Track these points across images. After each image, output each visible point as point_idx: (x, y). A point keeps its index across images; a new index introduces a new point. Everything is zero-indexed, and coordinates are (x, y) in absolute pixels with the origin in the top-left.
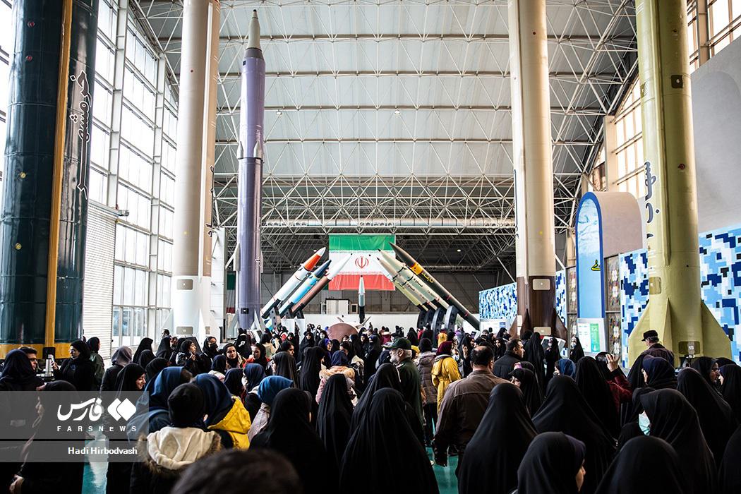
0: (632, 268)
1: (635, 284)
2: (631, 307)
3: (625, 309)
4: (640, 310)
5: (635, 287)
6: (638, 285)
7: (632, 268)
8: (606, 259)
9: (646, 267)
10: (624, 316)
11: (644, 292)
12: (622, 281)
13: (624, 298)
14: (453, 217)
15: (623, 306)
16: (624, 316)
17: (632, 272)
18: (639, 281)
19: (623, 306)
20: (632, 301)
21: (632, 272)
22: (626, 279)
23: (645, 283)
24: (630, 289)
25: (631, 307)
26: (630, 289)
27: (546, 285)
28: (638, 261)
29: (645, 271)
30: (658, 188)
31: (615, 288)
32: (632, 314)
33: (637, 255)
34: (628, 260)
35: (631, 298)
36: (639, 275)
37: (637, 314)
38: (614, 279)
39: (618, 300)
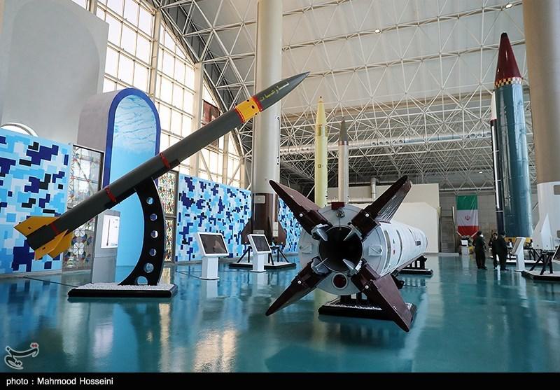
0: (191, 188)
1: (193, 199)
2: (188, 215)
3: (182, 216)
4: (195, 218)
5: (192, 201)
6: (196, 200)
7: (191, 188)
9: (203, 191)
10: (180, 221)
11: (200, 207)
12: (180, 194)
15: (180, 213)
16: (180, 221)
18: (196, 200)
19: (180, 213)
20: (189, 211)
22: (185, 194)
23: (201, 201)
24: (188, 203)
25: (188, 215)
26: (188, 203)
27: (262, 200)
29: (202, 194)
32: (187, 220)
33: (196, 181)
35: (188, 208)
37: (192, 221)
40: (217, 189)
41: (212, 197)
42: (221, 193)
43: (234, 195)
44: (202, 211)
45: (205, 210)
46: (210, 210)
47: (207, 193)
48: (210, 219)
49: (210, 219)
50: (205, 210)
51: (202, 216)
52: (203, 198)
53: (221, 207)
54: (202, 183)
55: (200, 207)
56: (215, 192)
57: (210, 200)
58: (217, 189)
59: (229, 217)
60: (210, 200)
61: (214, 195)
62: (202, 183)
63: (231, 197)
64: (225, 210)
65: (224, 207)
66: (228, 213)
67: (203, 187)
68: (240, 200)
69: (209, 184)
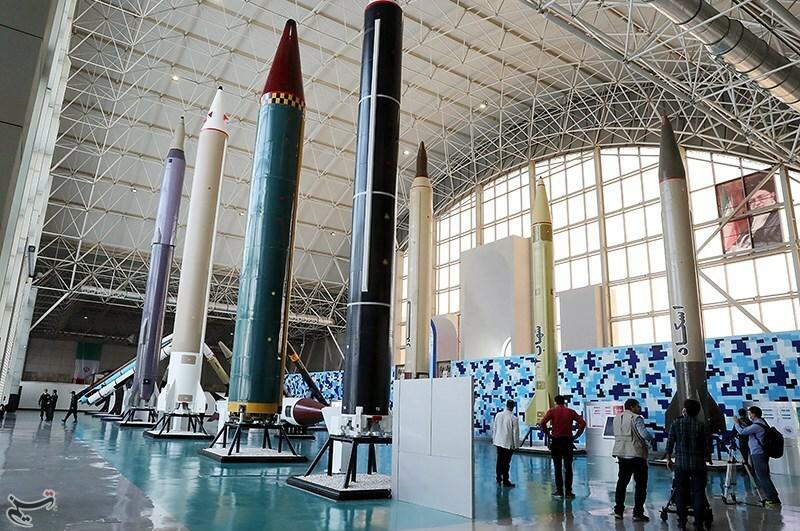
14: (313, 313)
28: (468, 367)
34: (458, 365)
41: (486, 375)
42: (497, 367)
43: (516, 365)
46: (484, 388)
47: (479, 371)
48: (484, 397)
49: (484, 397)
53: (498, 383)
54: (473, 364)
56: (488, 368)
57: (483, 378)
59: (509, 393)
60: (483, 378)
61: (488, 371)
62: (473, 364)
63: (512, 368)
64: (504, 384)
65: (502, 382)
66: (509, 389)
67: (474, 367)
68: (528, 369)
69: (482, 363)
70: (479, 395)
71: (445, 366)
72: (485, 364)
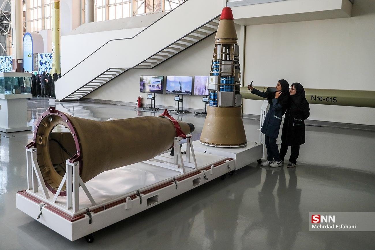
0: (42, 58)
2: (42, 68)
4: (44, 69)
5: (43, 63)
7: (42, 58)
8: (34, 54)
11: (46, 65)
13: (40, 66)
17: (42, 59)
21: (42, 59)
22: (40, 61)
23: (46, 62)
24: (41, 64)
25: (42, 68)
26: (41, 64)
28: (44, 56)
29: (46, 59)
30: (55, 48)
31: (37, 63)
34: (41, 55)
36: (44, 60)
38: (36, 60)
39: (38, 66)
40: (52, 56)
44: (46, 66)
45: (47, 66)
46: (50, 65)
47: (48, 58)
48: (50, 69)
50: (47, 66)
51: (47, 68)
52: (47, 61)
54: (46, 55)
55: (46, 65)
57: (49, 61)
58: (52, 56)
60: (49, 61)
61: (51, 58)
62: (46, 55)
67: (46, 56)
69: (49, 54)
70: (48, 68)
71: (36, 55)
72: (50, 55)
